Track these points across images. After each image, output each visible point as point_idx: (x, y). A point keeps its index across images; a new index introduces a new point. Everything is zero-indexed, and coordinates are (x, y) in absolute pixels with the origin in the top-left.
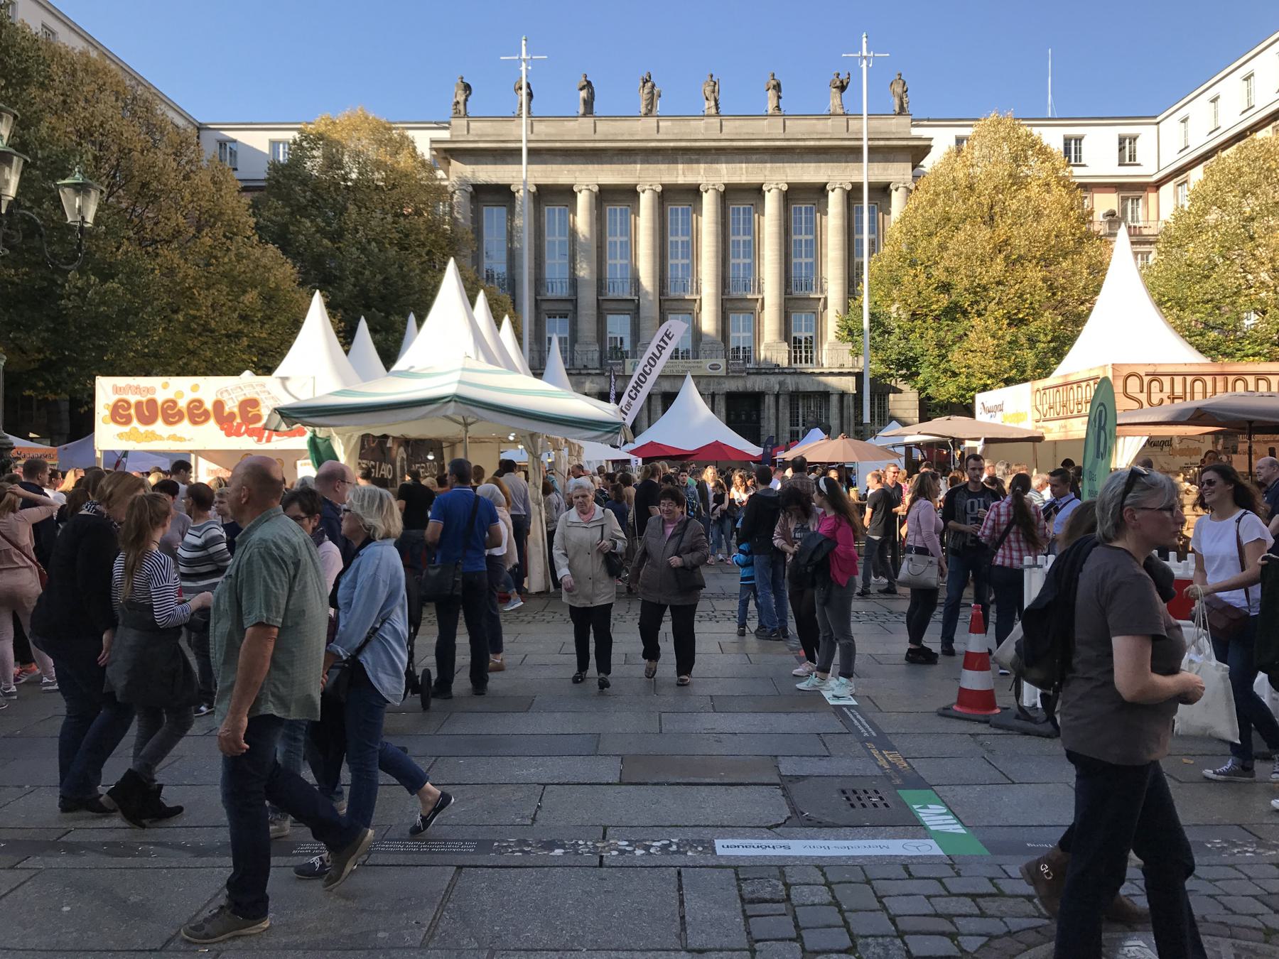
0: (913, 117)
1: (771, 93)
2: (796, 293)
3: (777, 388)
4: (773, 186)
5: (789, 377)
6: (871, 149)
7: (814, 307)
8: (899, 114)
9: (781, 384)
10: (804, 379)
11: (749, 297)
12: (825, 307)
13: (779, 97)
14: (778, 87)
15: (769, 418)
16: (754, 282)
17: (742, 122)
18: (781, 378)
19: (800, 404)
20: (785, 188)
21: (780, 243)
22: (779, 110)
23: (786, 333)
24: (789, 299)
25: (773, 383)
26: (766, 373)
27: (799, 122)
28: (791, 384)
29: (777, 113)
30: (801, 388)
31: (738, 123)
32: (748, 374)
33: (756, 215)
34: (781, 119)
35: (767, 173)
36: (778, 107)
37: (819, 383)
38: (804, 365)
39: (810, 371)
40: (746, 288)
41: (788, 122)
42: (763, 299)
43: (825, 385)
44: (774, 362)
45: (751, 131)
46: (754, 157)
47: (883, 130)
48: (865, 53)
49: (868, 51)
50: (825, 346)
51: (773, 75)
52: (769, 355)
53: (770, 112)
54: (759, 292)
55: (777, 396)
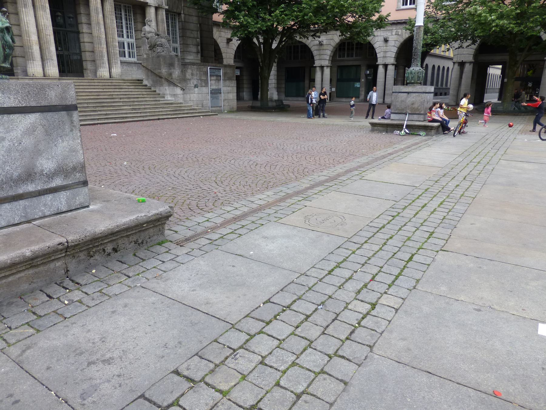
15: (98, 23)
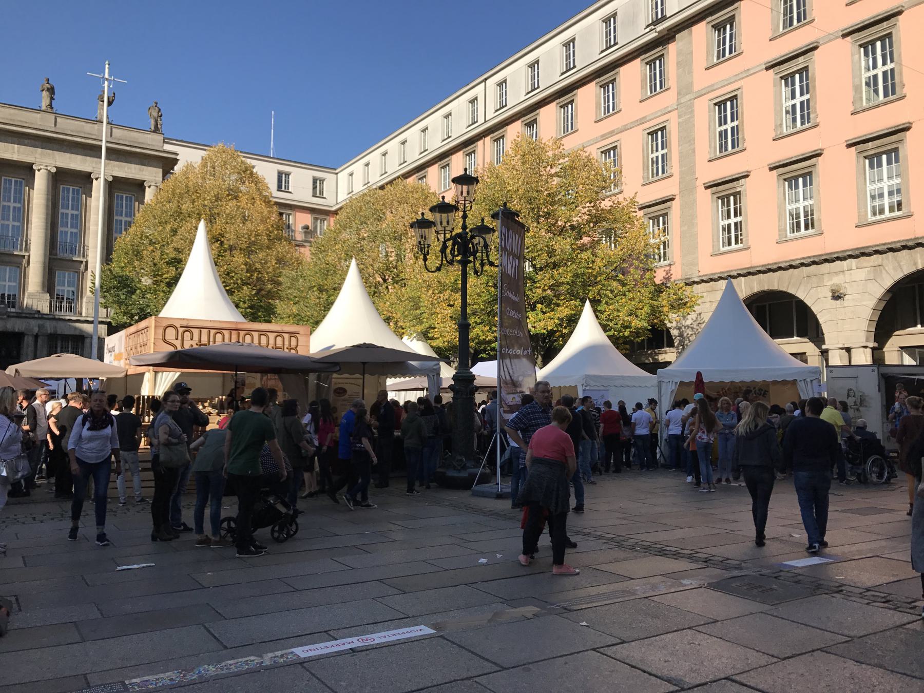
0: (165, 136)
1: (45, 94)
2: (61, 255)
3: (36, 330)
4: (42, 167)
5: (48, 321)
6: (108, 149)
7: (77, 269)
8: (154, 132)
9: (40, 327)
10: (61, 324)
11: (15, 253)
12: (86, 269)
13: (52, 99)
14: (51, 90)
16: (22, 241)
17: (17, 111)
18: (40, 322)
19: (70, 345)
20: (54, 170)
21: (47, 214)
22: (52, 108)
23: (49, 285)
24: (54, 259)
25: (34, 326)
26: (26, 317)
27: (68, 121)
28: (49, 327)
29: (49, 110)
30: (59, 332)
31: (12, 111)
32: (9, 316)
33: (27, 188)
34: (53, 116)
35: (37, 156)
36: (51, 106)
37: (76, 328)
38: (57, 313)
39: (68, 318)
40: (14, 246)
41: (59, 120)
42: (29, 256)
43: (81, 330)
44: (35, 308)
45: (25, 120)
46: (26, 141)
47: (140, 141)
48: (107, 76)
49: (110, 75)
50: (84, 300)
51: (48, 80)
52: (30, 302)
53: (44, 108)
54: (26, 250)
55: (36, 337)
